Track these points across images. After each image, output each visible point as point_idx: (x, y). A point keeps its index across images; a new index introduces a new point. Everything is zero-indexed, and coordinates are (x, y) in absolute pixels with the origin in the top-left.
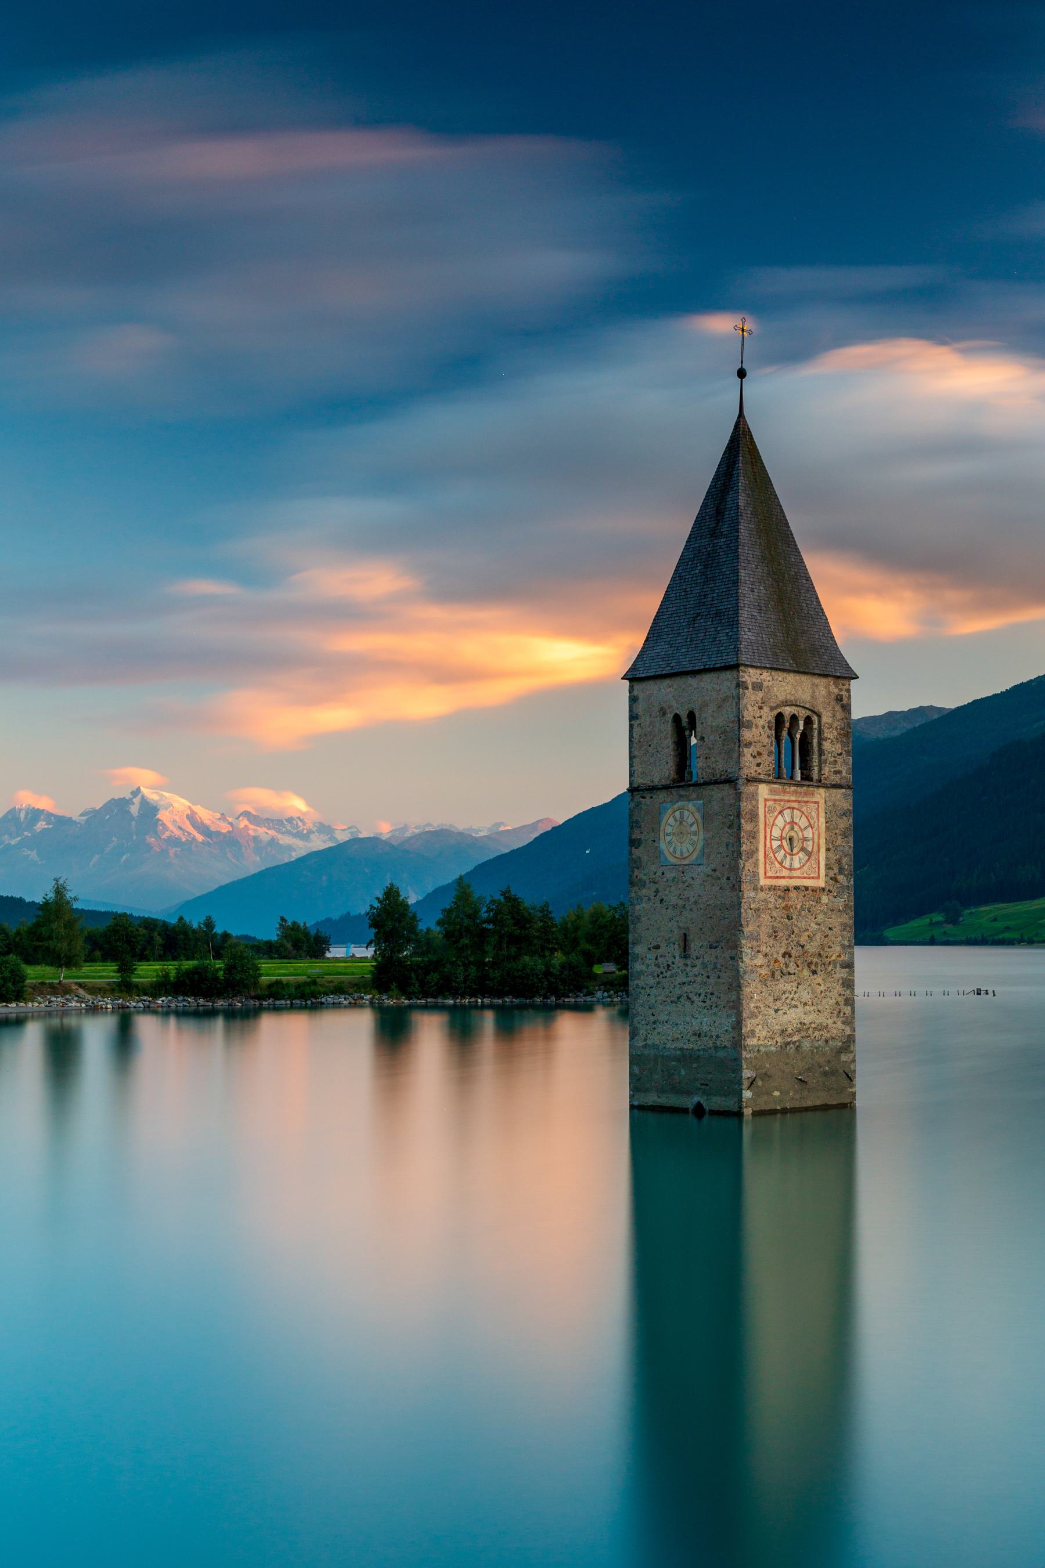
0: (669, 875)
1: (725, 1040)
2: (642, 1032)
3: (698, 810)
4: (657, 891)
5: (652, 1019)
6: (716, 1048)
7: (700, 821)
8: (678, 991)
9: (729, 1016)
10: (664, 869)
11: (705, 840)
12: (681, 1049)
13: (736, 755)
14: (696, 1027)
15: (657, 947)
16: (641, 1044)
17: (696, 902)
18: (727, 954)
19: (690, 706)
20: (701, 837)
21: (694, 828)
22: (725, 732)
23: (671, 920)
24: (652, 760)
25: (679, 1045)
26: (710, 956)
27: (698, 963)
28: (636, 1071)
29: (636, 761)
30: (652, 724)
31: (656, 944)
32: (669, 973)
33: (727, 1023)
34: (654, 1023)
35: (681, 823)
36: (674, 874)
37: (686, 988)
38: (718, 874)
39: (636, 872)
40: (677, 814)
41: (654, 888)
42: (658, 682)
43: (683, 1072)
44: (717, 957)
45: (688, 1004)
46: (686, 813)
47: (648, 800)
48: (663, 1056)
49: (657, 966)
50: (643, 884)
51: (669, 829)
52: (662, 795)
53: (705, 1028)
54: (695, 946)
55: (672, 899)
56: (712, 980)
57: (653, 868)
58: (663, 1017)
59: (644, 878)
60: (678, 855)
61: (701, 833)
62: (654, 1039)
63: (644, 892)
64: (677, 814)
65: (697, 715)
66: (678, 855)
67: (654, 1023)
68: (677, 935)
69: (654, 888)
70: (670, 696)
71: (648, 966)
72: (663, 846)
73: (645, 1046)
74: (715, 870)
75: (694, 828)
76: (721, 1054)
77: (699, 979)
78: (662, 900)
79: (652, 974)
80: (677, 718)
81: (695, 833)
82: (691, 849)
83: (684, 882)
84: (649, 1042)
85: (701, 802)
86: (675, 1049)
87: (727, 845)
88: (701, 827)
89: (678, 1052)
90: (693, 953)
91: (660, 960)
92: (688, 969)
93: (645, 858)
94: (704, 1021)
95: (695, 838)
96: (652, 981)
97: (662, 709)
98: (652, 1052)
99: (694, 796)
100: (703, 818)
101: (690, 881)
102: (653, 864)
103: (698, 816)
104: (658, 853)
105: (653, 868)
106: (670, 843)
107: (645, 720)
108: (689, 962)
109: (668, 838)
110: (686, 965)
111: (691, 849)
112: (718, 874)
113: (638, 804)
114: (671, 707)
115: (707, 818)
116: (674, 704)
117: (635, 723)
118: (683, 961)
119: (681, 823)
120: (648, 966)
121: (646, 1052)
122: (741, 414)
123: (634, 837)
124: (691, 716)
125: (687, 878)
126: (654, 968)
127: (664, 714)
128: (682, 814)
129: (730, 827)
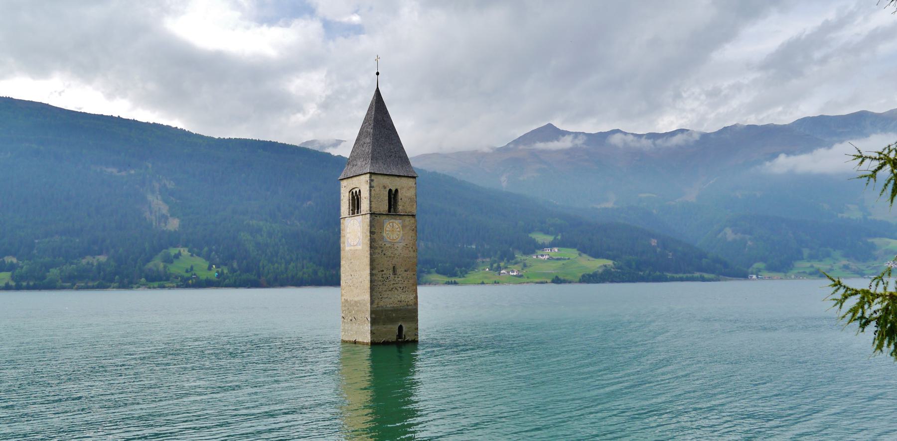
0: (388, 245)
1: (411, 303)
2: (376, 302)
3: (400, 224)
4: (382, 251)
5: (381, 297)
6: (407, 305)
7: (401, 228)
8: (392, 286)
9: (412, 294)
10: (385, 243)
11: (403, 234)
12: (394, 307)
13: (415, 207)
14: (399, 299)
15: (383, 271)
16: (376, 306)
17: (399, 255)
18: (412, 274)
19: (397, 187)
20: (401, 233)
21: (398, 230)
22: (410, 199)
23: (388, 261)
24: (380, 203)
25: (391, 305)
26: (405, 274)
27: (400, 276)
28: (373, 316)
29: (373, 203)
30: (380, 190)
31: (382, 270)
32: (388, 280)
33: (412, 297)
34: (381, 298)
35: (393, 227)
36: (389, 245)
37: (395, 285)
38: (407, 246)
39: (373, 243)
40: (391, 224)
41: (381, 250)
42: (383, 176)
43: (394, 315)
44: (407, 275)
45: (396, 291)
46: (395, 224)
47: (378, 218)
48: (385, 310)
49: (383, 278)
50: (377, 248)
51: (387, 229)
52: (384, 217)
53: (403, 299)
54: (399, 271)
55: (389, 253)
56: (406, 282)
57: (380, 243)
58: (386, 296)
59: (377, 246)
60: (391, 238)
61: (401, 231)
62: (381, 304)
63: (376, 251)
64: (391, 224)
65: (399, 190)
66: (391, 238)
67: (381, 298)
68: (391, 266)
69: (381, 250)
70: (388, 182)
71: (378, 278)
72: (384, 235)
73: (378, 307)
74: (407, 245)
75: (398, 230)
76: (410, 307)
77: (400, 282)
78: (384, 254)
79: (380, 281)
80: (390, 191)
81: (399, 231)
82: (397, 237)
83: (394, 248)
84: (379, 305)
85: (401, 221)
86: (391, 307)
87: (412, 236)
88: (401, 230)
89: (392, 308)
90: (398, 273)
91: (383, 275)
92: (396, 278)
93: (377, 239)
94: (403, 297)
95: (399, 233)
96: (380, 283)
97: (384, 186)
98: (380, 309)
99: (398, 218)
100: (402, 226)
101: (396, 248)
102: (381, 241)
103: (400, 226)
104: (383, 238)
105: (380, 243)
106: (388, 234)
107: (377, 189)
108: (396, 276)
109: (387, 232)
110: (395, 277)
111: (397, 237)
112: (407, 246)
113: (373, 219)
114: (388, 186)
115: (404, 227)
116: (390, 186)
117: (373, 189)
118: (393, 276)
119: (393, 227)
120: (378, 278)
121: (378, 309)
122: (378, 88)
123: (372, 230)
124: (397, 191)
125: (396, 247)
126: (382, 279)
127: (385, 188)
128: (393, 225)
129: (413, 231)
